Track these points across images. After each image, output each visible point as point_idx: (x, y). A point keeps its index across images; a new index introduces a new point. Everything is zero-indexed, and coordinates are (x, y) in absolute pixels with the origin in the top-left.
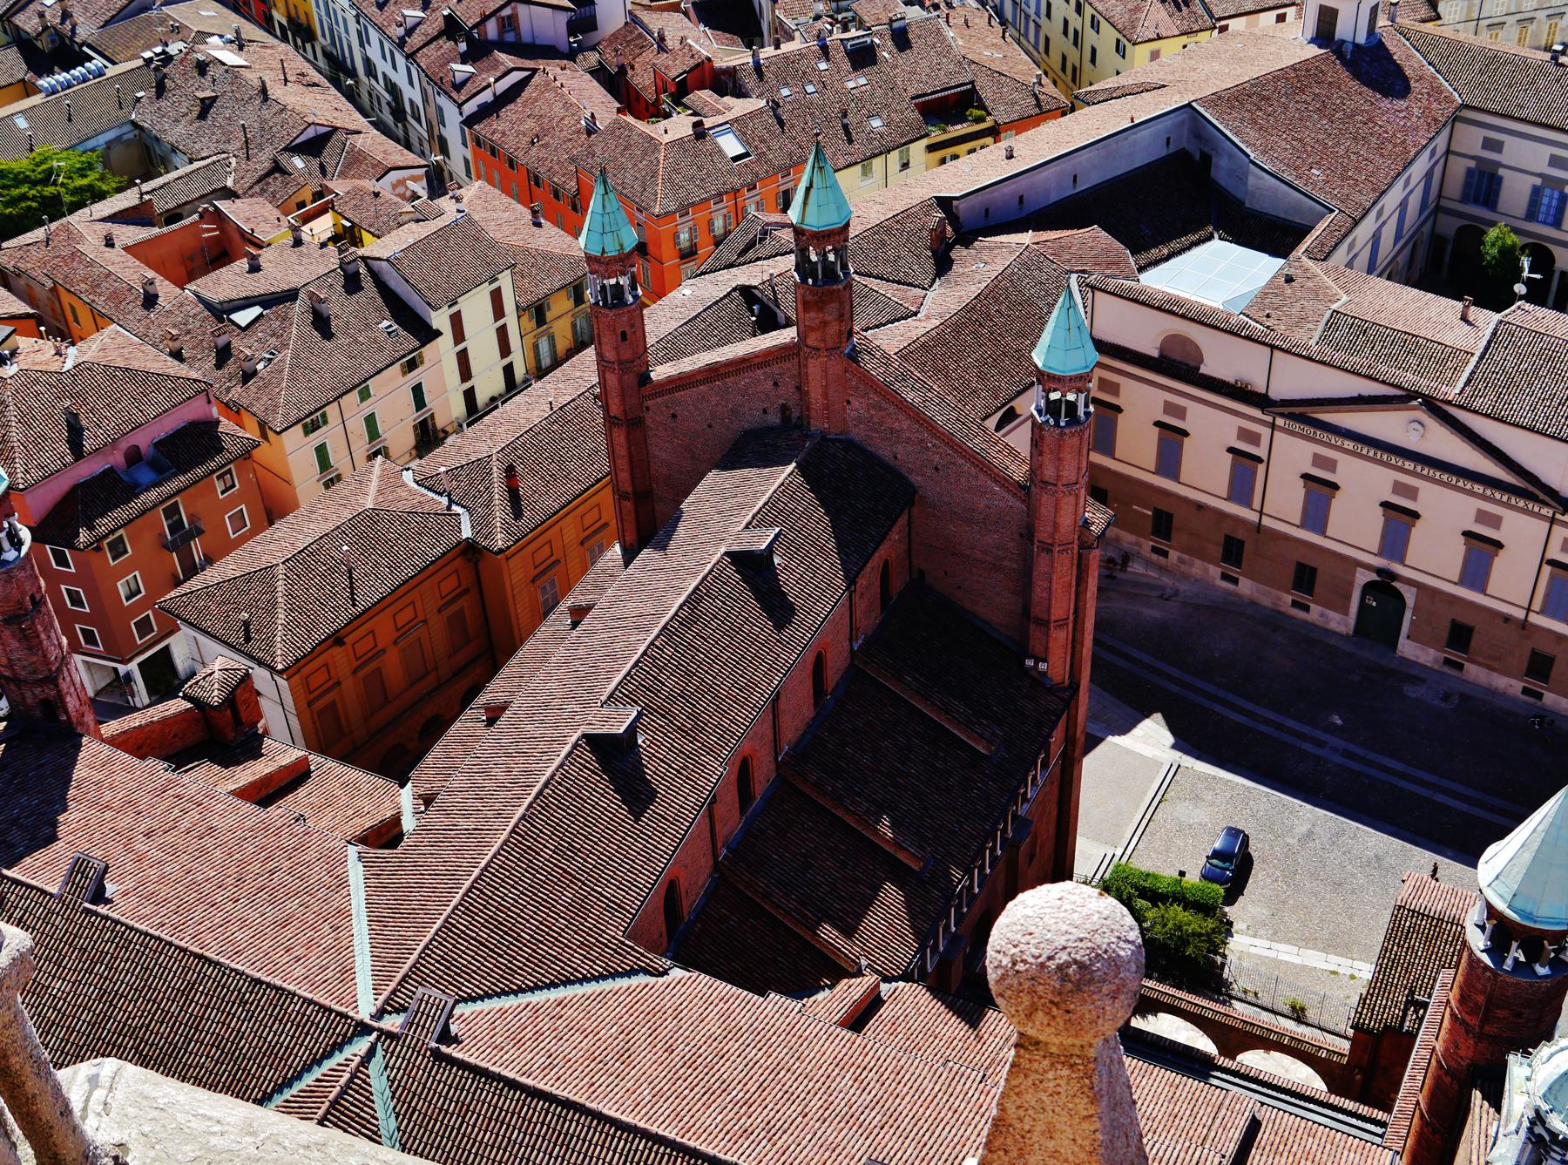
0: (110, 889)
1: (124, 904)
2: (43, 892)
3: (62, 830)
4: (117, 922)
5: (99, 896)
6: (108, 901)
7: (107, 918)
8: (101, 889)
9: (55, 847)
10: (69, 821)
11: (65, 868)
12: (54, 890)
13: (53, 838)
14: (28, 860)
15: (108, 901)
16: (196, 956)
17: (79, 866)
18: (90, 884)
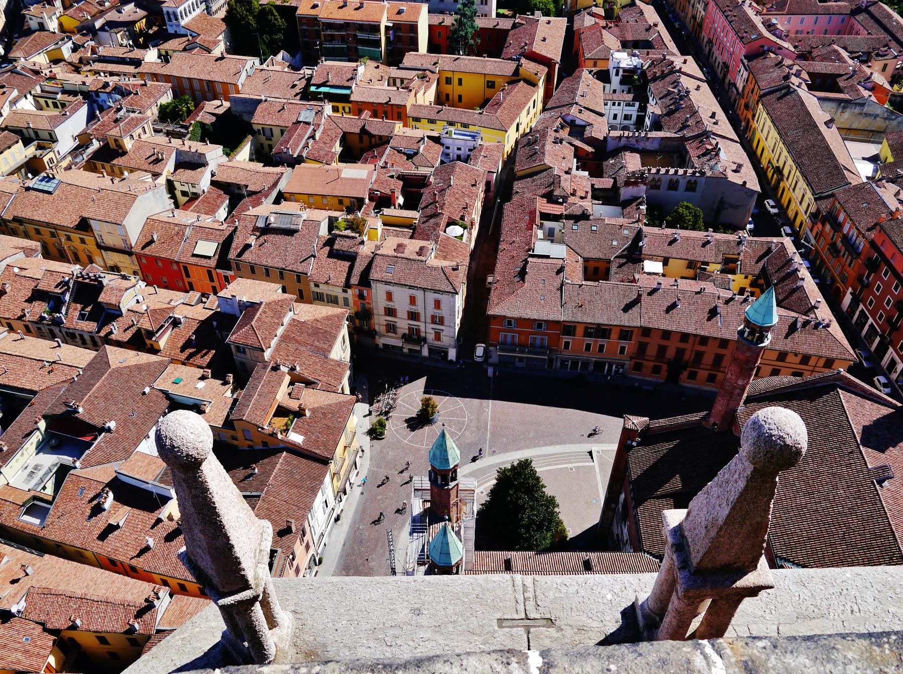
0: (886, 484)
1: (886, 491)
2: (866, 464)
3: (888, 452)
4: (878, 495)
5: (880, 482)
6: (881, 486)
7: (876, 490)
8: (883, 481)
9: (881, 454)
10: (892, 452)
11: (879, 465)
12: (870, 467)
13: (883, 452)
14: (870, 450)
15: (881, 486)
16: (892, 530)
17: (884, 468)
18: (883, 475)
